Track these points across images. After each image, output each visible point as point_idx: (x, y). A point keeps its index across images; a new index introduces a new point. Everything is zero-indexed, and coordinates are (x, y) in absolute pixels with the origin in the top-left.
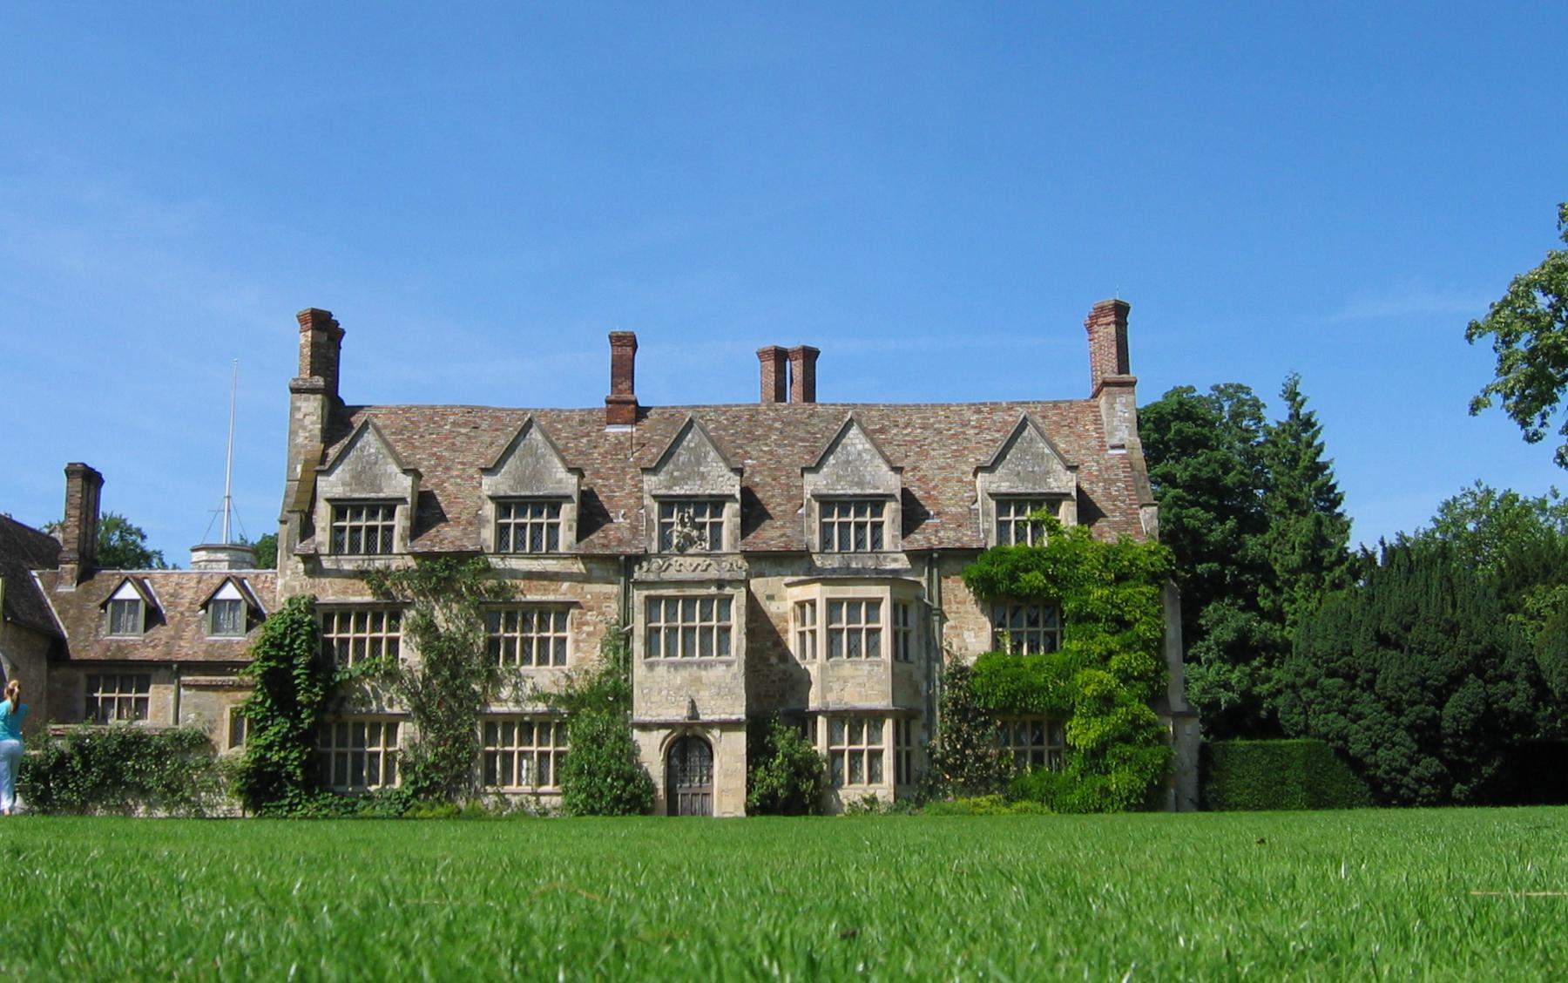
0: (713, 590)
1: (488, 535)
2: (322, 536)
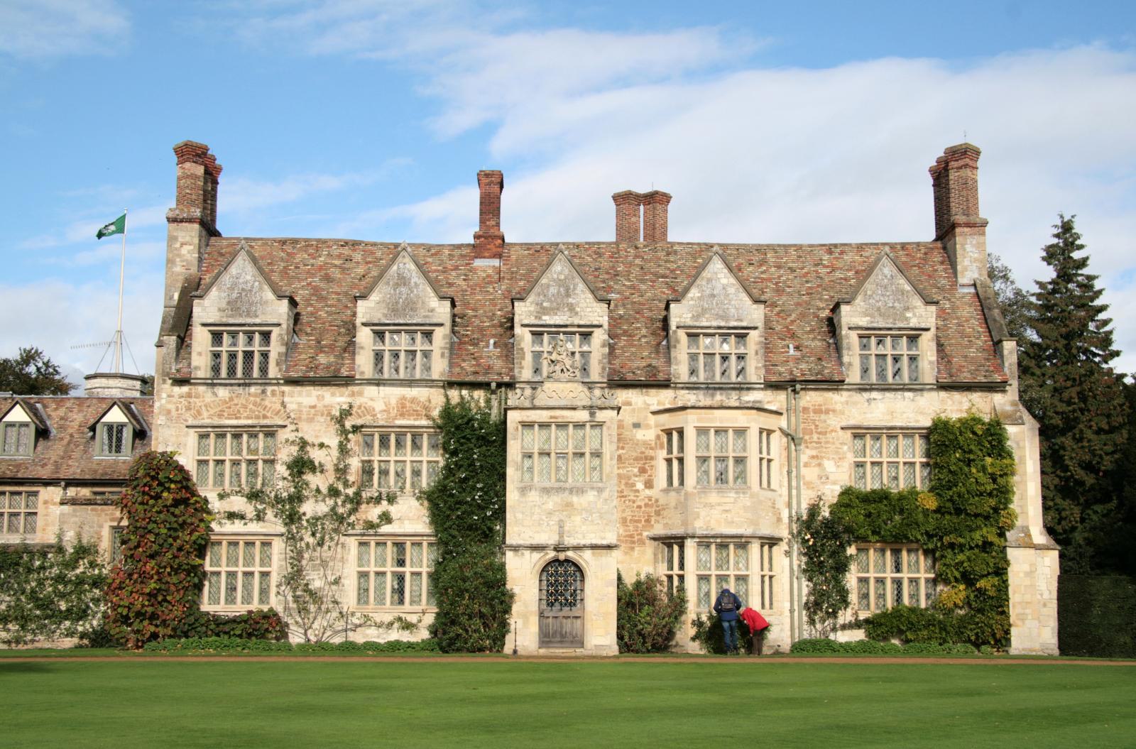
0: (583, 416)
2: (200, 359)
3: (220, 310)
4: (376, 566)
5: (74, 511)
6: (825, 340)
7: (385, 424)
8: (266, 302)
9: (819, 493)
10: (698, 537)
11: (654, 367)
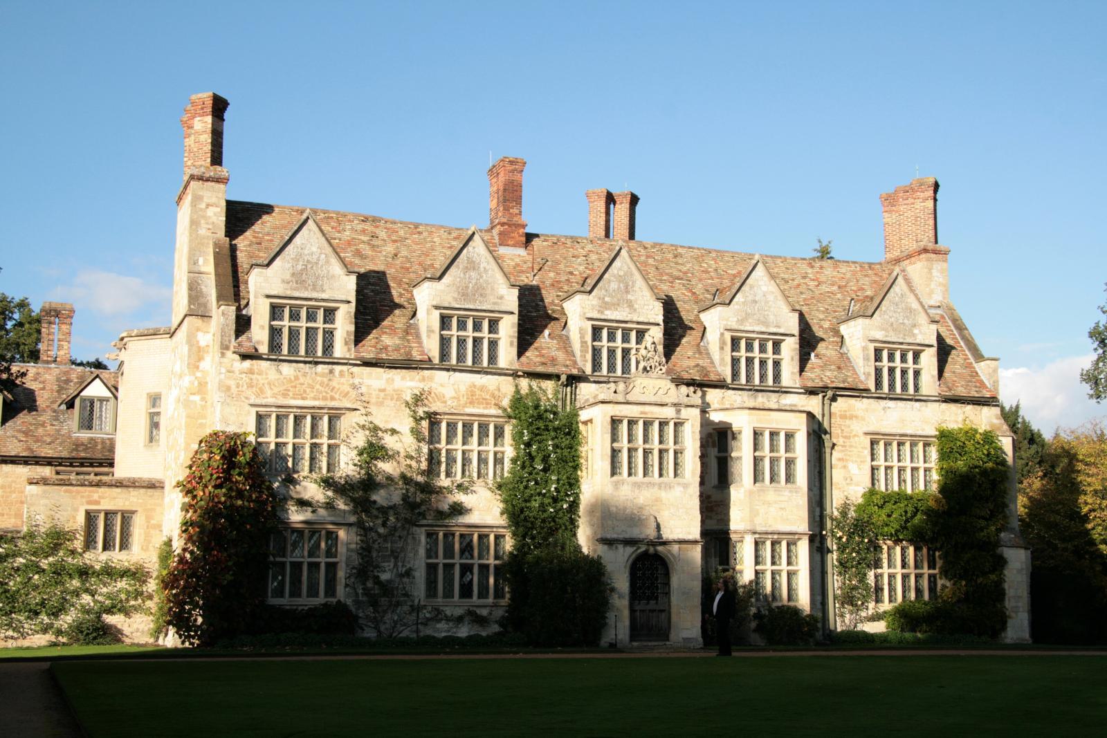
0: (669, 413)
1: (432, 347)
2: (259, 334)
3: (283, 281)
4: (445, 558)
5: (44, 492)
6: (836, 350)
7: (455, 412)
8: (333, 276)
9: (846, 493)
10: (759, 533)
11: (702, 367)
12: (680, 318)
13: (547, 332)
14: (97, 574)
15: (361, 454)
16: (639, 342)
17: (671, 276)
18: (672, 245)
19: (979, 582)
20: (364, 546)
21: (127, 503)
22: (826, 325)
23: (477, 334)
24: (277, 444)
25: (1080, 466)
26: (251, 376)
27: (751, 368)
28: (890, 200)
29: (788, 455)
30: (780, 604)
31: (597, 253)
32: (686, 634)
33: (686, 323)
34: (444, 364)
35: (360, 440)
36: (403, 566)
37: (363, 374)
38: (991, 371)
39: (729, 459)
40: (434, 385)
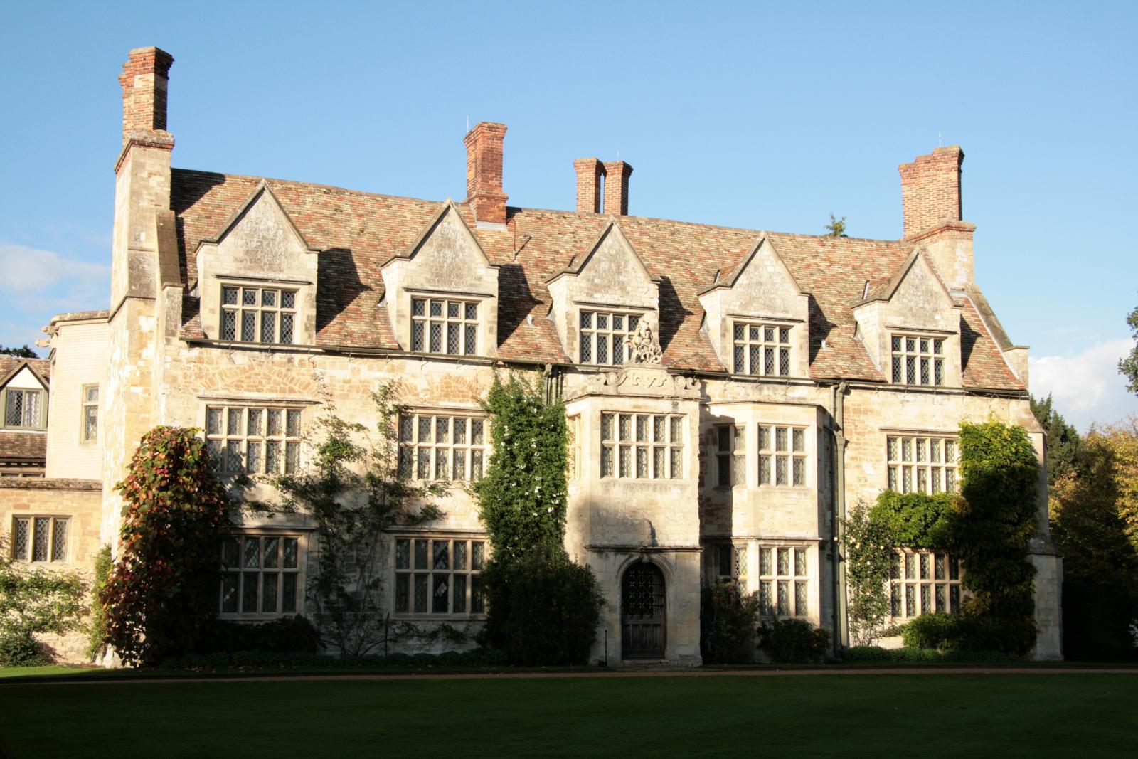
0: (664, 407)
2: (209, 319)
3: (236, 260)
4: (417, 567)
7: (429, 405)
8: (292, 254)
9: (859, 496)
11: (702, 356)
12: (678, 302)
13: (530, 317)
14: (26, 587)
15: (323, 452)
16: (631, 329)
17: (668, 255)
18: (669, 221)
19: (1005, 592)
20: (327, 554)
21: (60, 507)
22: (839, 309)
23: (453, 320)
24: (229, 441)
25: (1118, 466)
26: (200, 365)
27: (755, 355)
28: (910, 172)
29: (797, 453)
30: (786, 618)
31: (586, 230)
32: (682, 651)
33: (684, 307)
34: (415, 351)
35: (323, 436)
36: (370, 577)
37: (325, 363)
38: (1020, 360)
39: (731, 458)
40: (405, 376)
